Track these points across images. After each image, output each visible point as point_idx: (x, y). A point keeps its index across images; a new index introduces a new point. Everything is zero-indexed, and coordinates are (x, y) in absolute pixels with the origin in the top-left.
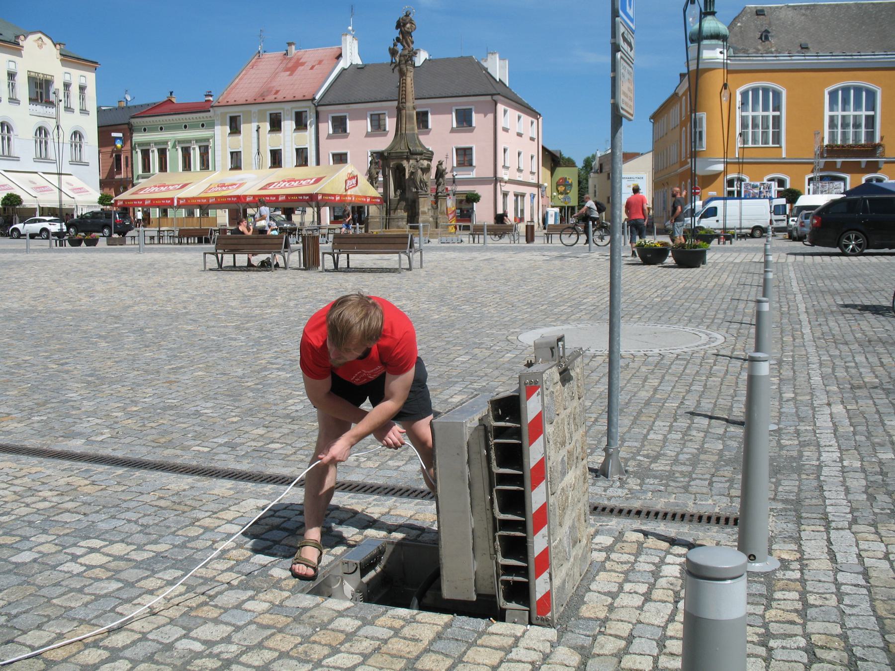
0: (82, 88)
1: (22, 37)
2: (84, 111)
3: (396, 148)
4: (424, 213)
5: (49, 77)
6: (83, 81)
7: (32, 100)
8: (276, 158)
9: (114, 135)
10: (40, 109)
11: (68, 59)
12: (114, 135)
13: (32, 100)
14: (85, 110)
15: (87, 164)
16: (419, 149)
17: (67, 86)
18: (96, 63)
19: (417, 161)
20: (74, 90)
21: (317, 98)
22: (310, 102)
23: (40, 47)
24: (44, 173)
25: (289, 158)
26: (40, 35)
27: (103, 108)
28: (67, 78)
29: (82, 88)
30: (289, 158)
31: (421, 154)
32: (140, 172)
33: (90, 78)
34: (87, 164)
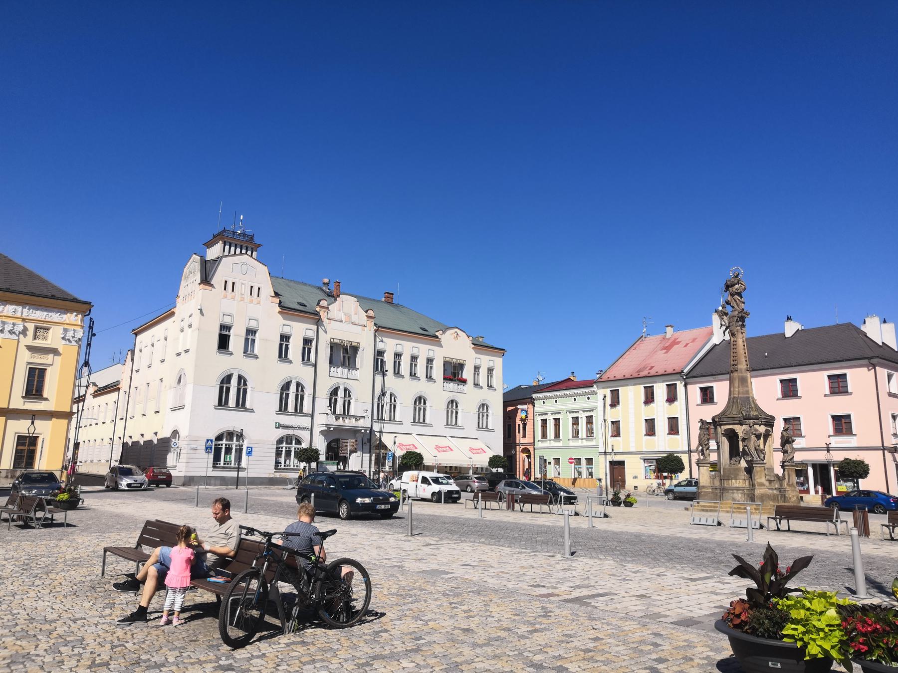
0: (490, 370)
2: (490, 386)
3: (728, 413)
4: (762, 485)
5: (461, 362)
6: (491, 364)
7: (446, 379)
8: (650, 427)
10: (452, 386)
11: (479, 346)
13: (446, 379)
14: (477, 384)
15: (493, 431)
16: (754, 413)
17: (477, 368)
18: (504, 350)
19: (750, 427)
20: (483, 372)
21: (685, 371)
22: (679, 375)
24: (451, 437)
25: (662, 426)
26: (457, 330)
27: (523, 387)
28: (478, 362)
29: (490, 370)
30: (662, 426)
31: (757, 418)
32: (540, 438)
33: (497, 362)
34: (493, 431)
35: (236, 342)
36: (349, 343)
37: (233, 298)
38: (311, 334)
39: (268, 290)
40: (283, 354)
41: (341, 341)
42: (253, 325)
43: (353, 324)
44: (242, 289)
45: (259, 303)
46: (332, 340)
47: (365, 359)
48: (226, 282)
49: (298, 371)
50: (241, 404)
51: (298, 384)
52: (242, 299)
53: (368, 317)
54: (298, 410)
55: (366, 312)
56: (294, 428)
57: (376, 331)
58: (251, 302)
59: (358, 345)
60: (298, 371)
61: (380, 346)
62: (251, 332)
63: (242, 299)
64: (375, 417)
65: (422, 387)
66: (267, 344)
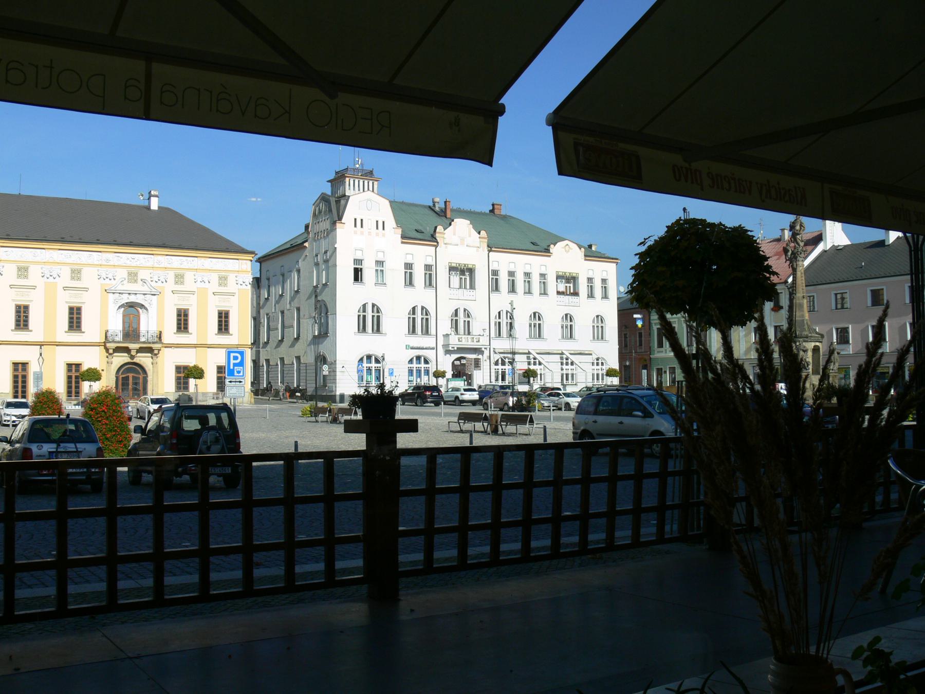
1: (552, 246)
9: (635, 316)
12: (635, 316)
23: (567, 252)
35: (369, 274)
36: (465, 266)
37: (362, 233)
38: (430, 261)
39: (391, 222)
40: (409, 281)
41: (458, 265)
42: (380, 257)
43: (467, 246)
44: (369, 224)
45: (384, 235)
46: (450, 264)
47: (482, 278)
48: (355, 219)
49: (421, 296)
50: (377, 329)
51: (423, 308)
52: (370, 233)
53: (480, 238)
54: (426, 332)
55: (479, 233)
56: (423, 349)
57: (489, 251)
58: (377, 235)
59: (474, 266)
60: (421, 296)
61: (494, 266)
62: (380, 263)
63: (370, 233)
64: (493, 335)
65: (535, 303)
66: (395, 274)
